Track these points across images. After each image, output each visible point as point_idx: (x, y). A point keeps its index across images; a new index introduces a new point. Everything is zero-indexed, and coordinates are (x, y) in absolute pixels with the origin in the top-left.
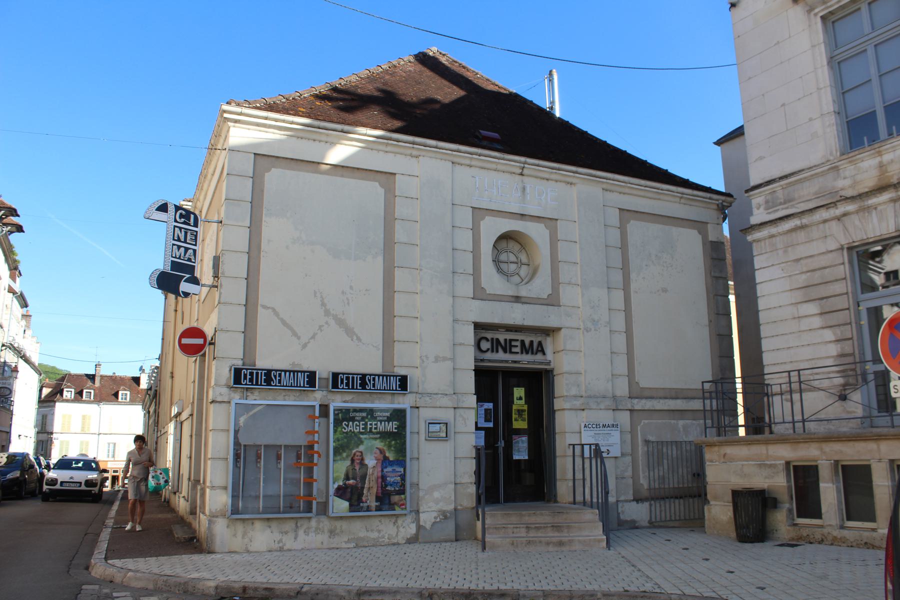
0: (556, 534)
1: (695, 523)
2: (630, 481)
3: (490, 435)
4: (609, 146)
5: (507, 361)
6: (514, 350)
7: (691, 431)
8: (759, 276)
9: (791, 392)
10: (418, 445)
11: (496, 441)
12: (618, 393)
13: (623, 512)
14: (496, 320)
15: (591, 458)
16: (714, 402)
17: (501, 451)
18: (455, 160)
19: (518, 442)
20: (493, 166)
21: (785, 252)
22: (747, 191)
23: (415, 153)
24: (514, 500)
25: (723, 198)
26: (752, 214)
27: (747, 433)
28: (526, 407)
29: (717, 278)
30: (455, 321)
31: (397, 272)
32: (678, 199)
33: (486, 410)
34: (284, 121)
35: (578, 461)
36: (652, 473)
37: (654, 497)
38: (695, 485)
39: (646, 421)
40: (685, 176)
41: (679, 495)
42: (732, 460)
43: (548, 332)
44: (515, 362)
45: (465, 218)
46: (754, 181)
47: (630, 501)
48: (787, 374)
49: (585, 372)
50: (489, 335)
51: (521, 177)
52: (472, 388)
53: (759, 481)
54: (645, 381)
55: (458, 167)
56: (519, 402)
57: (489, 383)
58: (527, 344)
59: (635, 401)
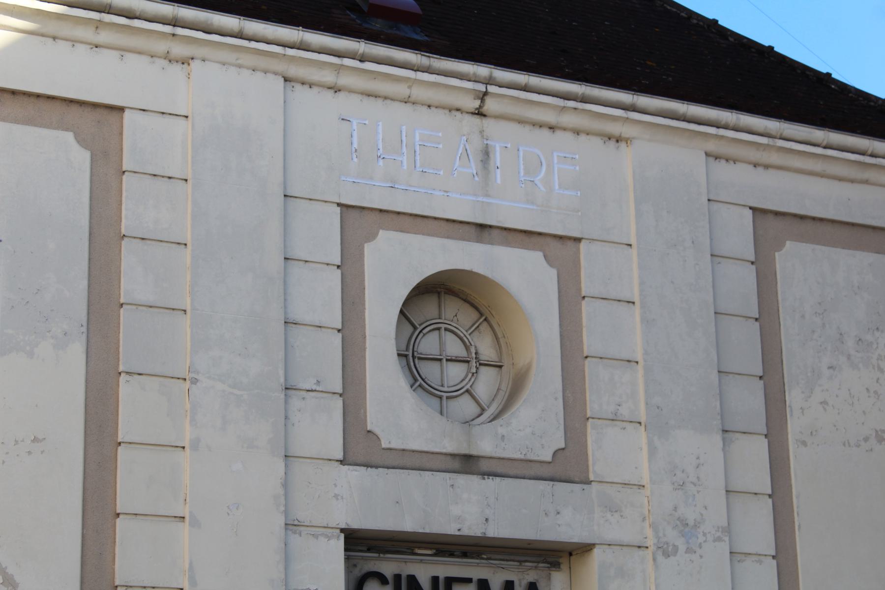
14: (408, 523)
18: (294, 71)
20: (401, 90)
23: (179, 50)
30: (291, 526)
31: (126, 388)
45: (321, 234)
50: (389, 567)
51: (476, 120)
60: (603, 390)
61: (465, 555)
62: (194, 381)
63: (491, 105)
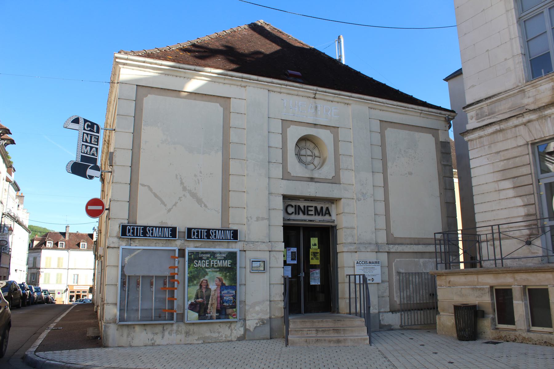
0: (336, 335)
1: (430, 326)
2: (388, 299)
3: (295, 269)
4: (374, 81)
5: (305, 220)
6: (310, 213)
7: (428, 266)
8: (473, 164)
9: (493, 240)
10: (245, 276)
11: (299, 272)
12: (380, 241)
13: (383, 320)
14: (298, 193)
15: (360, 284)
16: (443, 247)
17: (302, 279)
18: (270, 89)
19: (313, 274)
20: (296, 93)
21: (490, 147)
22: (464, 108)
23: (243, 84)
24: (310, 312)
25: (449, 113)
26: (467, 123)
27: (465, 267)
28: (319, 251)
29: (445, 165)
30: (270, 194)
31: (232, 162)
32: (419, 114)
33: (292, 252)
34: (156, 64)
35: (353, 285)
36: (402, 294)
37: (404, 309)
38: (431, 301)
39: (398, 260)
40: (424, 100)
41: (420, 308)
42: (454, 285)
43: (333, 201)
44: (311, 221)
45: (277, 127)
46: (469, 101)
47: (388, 312)
48: (490, 228)
49: (357, 227)
50: (293, 203)
51: (314, 100)
52: (281, 238)
53: (472, 299)
54: (398, 232)
55: (272, 93)
56: (314, 247)
57: (293, 234)
58: (319, 209)
59: (391, 246)
60: (344, 162)
61: (311, 201)
62: (247, 160)
63: (317, 96)
